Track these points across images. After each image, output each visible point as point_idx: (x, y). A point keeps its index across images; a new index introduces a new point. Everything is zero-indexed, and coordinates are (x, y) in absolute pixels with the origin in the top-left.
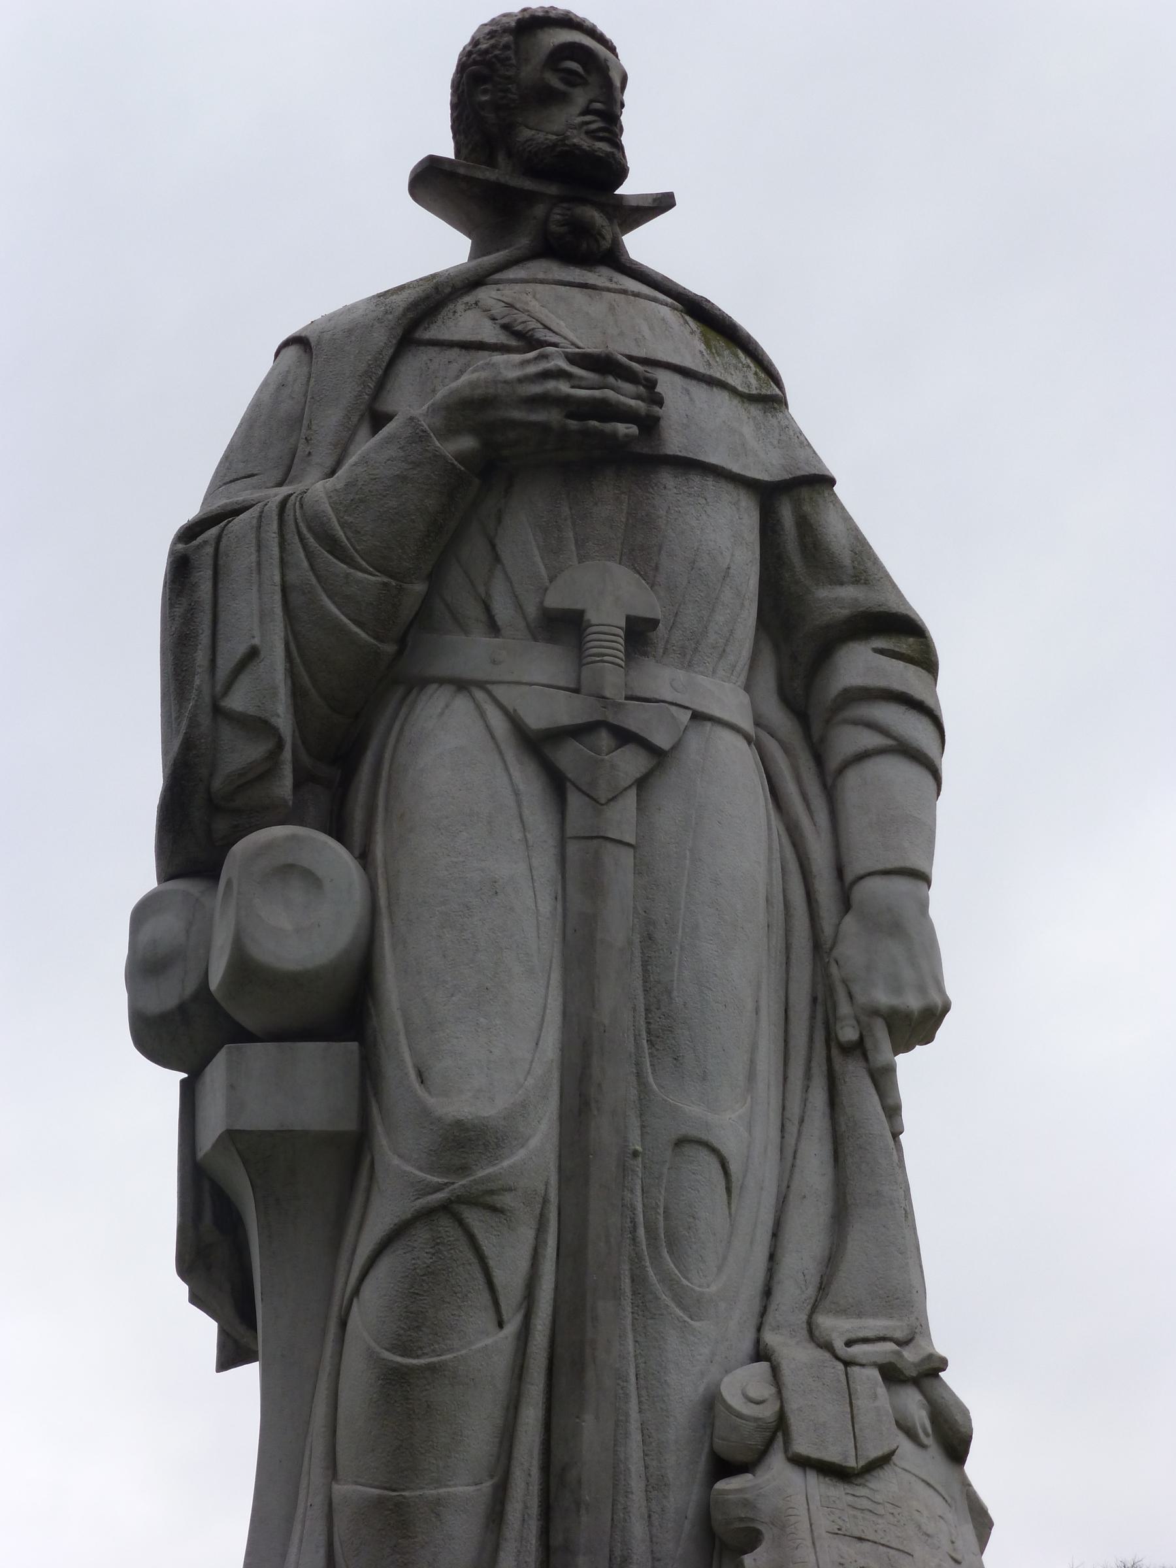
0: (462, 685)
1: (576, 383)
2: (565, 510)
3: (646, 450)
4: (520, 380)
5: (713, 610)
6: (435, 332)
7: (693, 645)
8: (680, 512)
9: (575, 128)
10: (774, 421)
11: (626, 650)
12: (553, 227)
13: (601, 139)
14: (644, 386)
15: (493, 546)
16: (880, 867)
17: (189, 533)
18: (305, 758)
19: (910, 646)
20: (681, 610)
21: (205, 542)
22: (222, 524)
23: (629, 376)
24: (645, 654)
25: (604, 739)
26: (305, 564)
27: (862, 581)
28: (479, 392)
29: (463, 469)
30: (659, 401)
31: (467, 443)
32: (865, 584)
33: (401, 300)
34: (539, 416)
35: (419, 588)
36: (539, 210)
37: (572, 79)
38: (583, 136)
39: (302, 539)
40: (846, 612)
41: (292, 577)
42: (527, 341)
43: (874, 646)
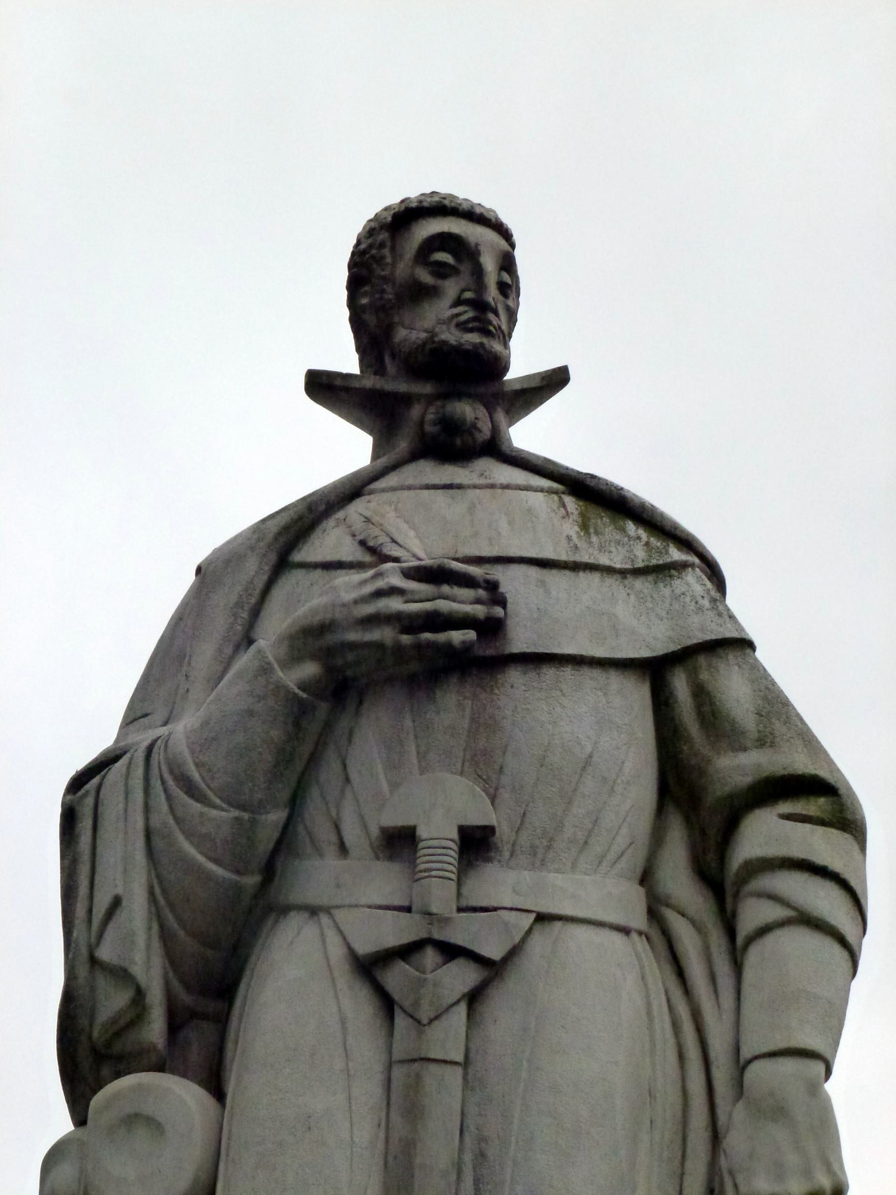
0: (313, 911)
1: (410, 597)
2: (408, 723)
3: (490, 652)
4: (356, 602)
5: (570, 802)
6: (298, 556)
7: (545, 843)
8: (528, 709)
9: (444, 323)
10: (667, 591)
11: (459, 863)
12: (428, 428)
13: (471, 330)
14: (485, 589)
15: (345, 766)
16: (765, 1049)
17: (78, 783)
18: (185, 998)
19: (820, 807)
20: (530, 809)
21: (87, 792)
22: (103, 773)
23: (467, 581)
24: (489, 860)
25: (430, 956)
26: (165, 808)
27: (768, 744)
28: (317, 619)
29: (304, 695)
30: (502, 602)
31: (310, 669)
32: (771, 746)
33: (274, 527)
34: (375, 635)
35: (276, 817)
36: (416, 411)
37: (442, 271)
38: (453, 330)
39: (163, 782)
40: (748, 780)
41: (156, 821)
42: (379, 556)
43: (781, 812)
